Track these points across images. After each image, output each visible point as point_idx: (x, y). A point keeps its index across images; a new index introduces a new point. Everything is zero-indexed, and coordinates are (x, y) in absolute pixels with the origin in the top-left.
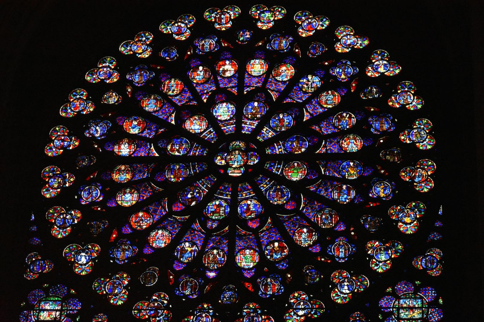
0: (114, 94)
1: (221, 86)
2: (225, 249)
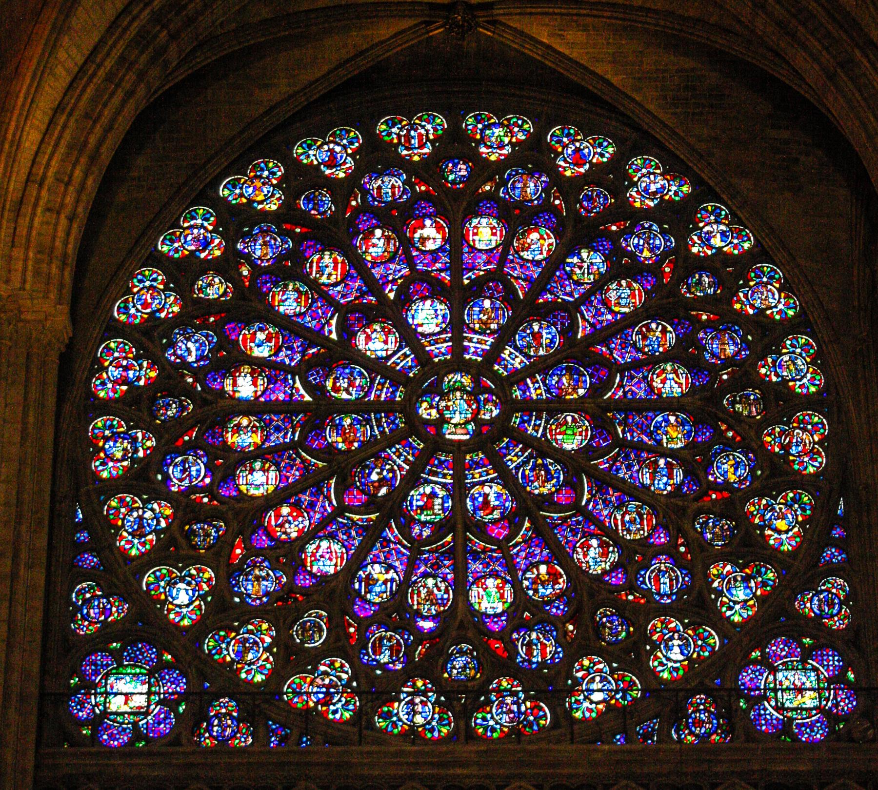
0: (217, 280)
2: (449, 577)
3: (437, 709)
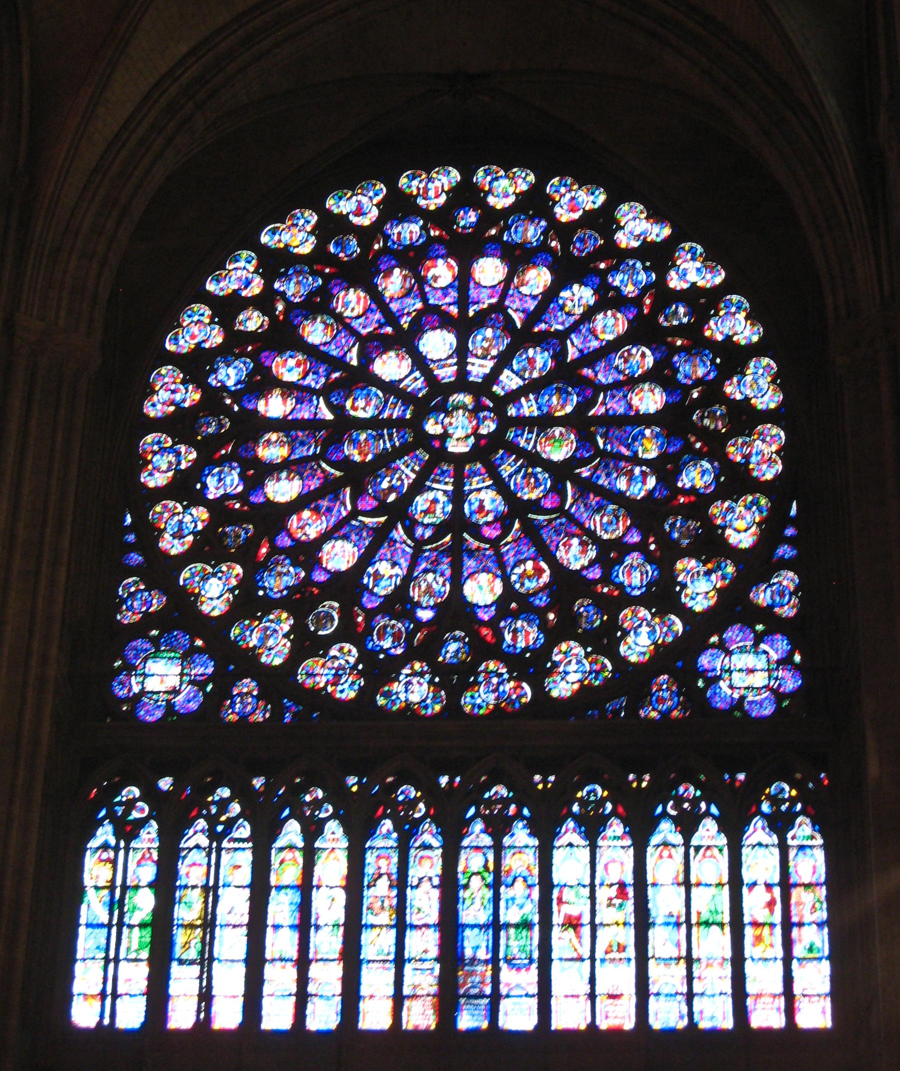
1: (431, 301)
3: (432, 689)
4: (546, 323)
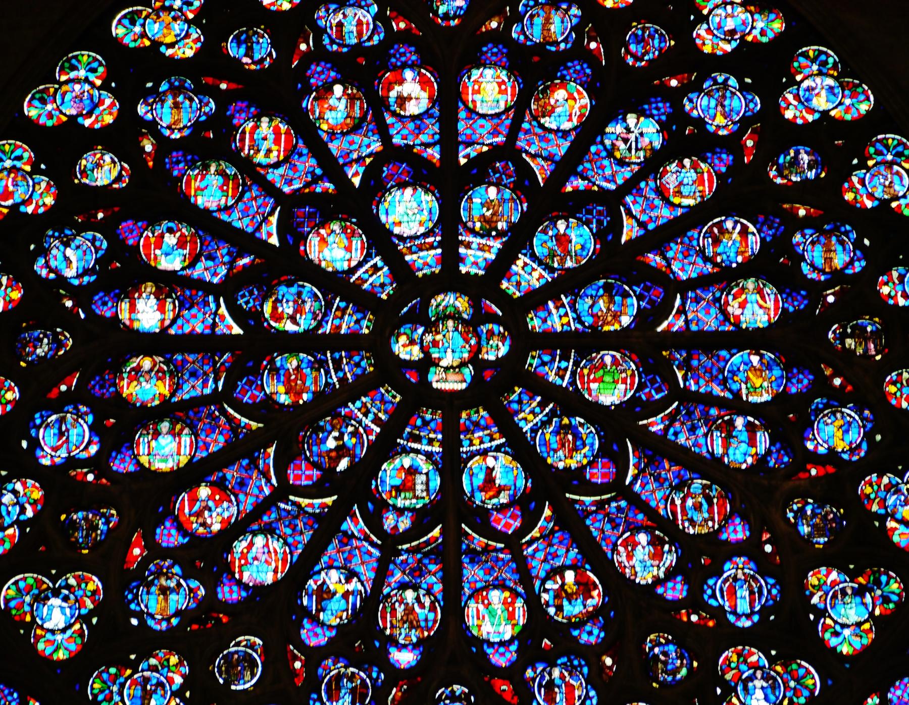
0: (107, 158)
1: (397, 140)
4: (583, 179)
